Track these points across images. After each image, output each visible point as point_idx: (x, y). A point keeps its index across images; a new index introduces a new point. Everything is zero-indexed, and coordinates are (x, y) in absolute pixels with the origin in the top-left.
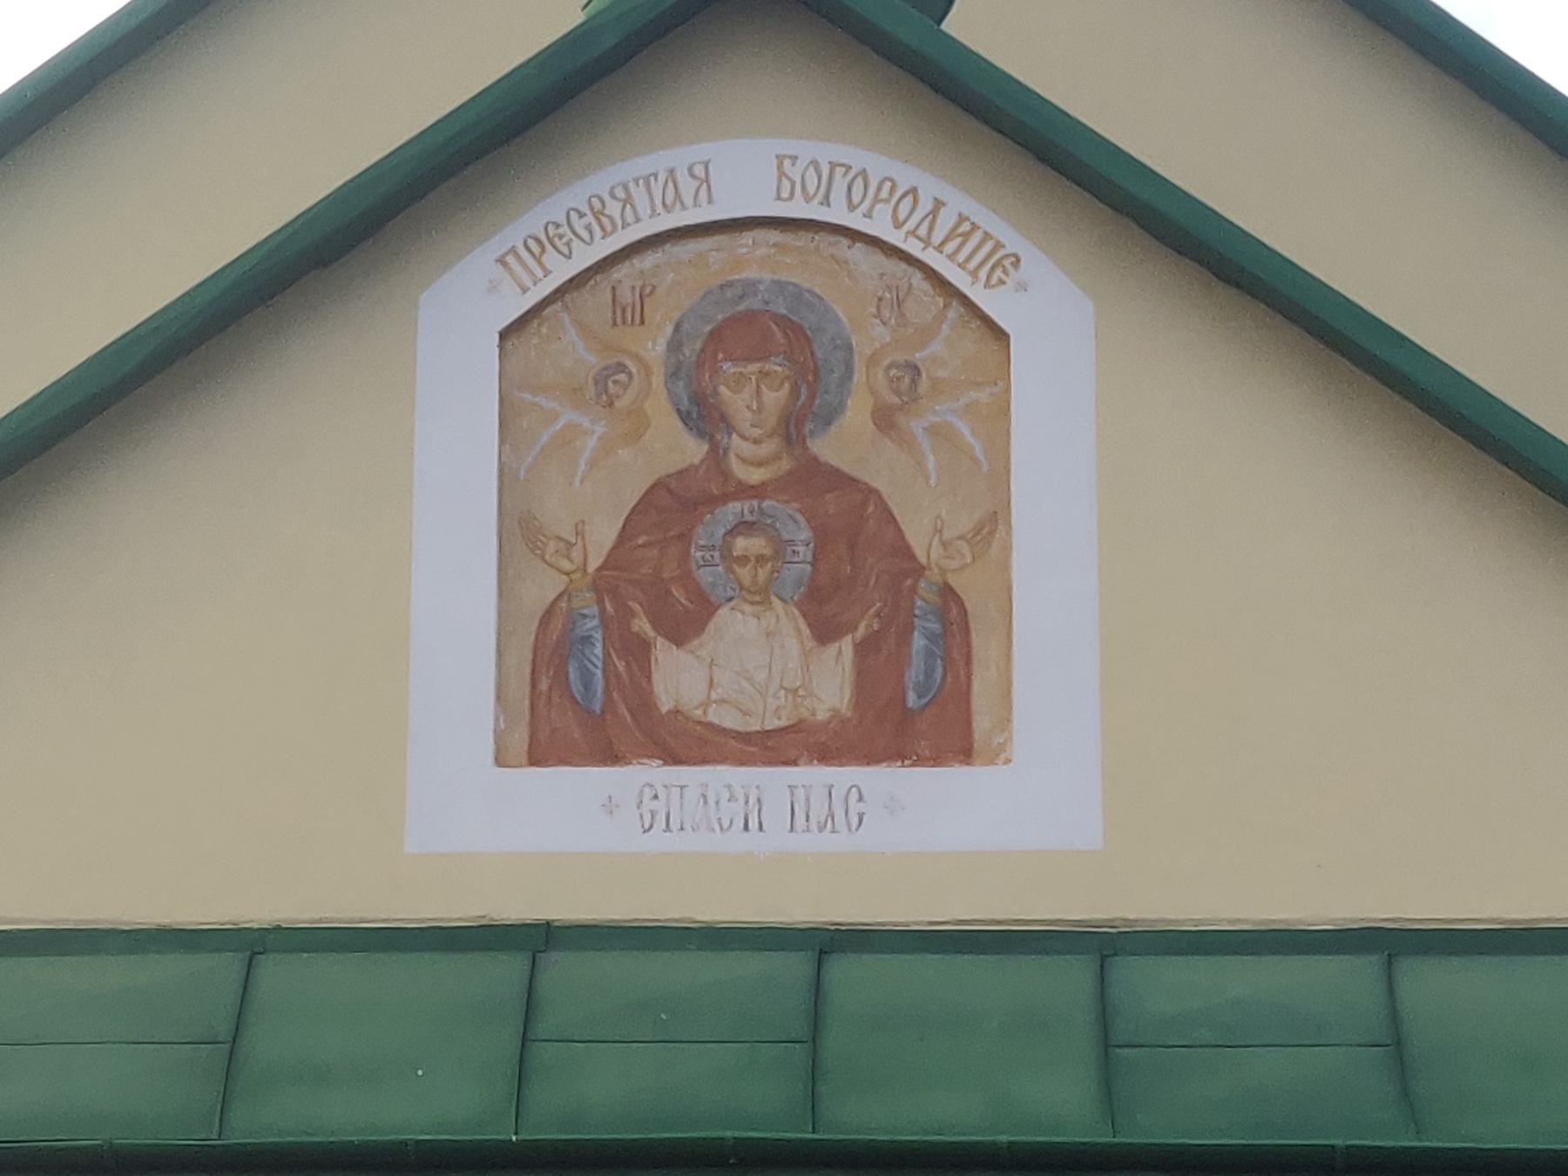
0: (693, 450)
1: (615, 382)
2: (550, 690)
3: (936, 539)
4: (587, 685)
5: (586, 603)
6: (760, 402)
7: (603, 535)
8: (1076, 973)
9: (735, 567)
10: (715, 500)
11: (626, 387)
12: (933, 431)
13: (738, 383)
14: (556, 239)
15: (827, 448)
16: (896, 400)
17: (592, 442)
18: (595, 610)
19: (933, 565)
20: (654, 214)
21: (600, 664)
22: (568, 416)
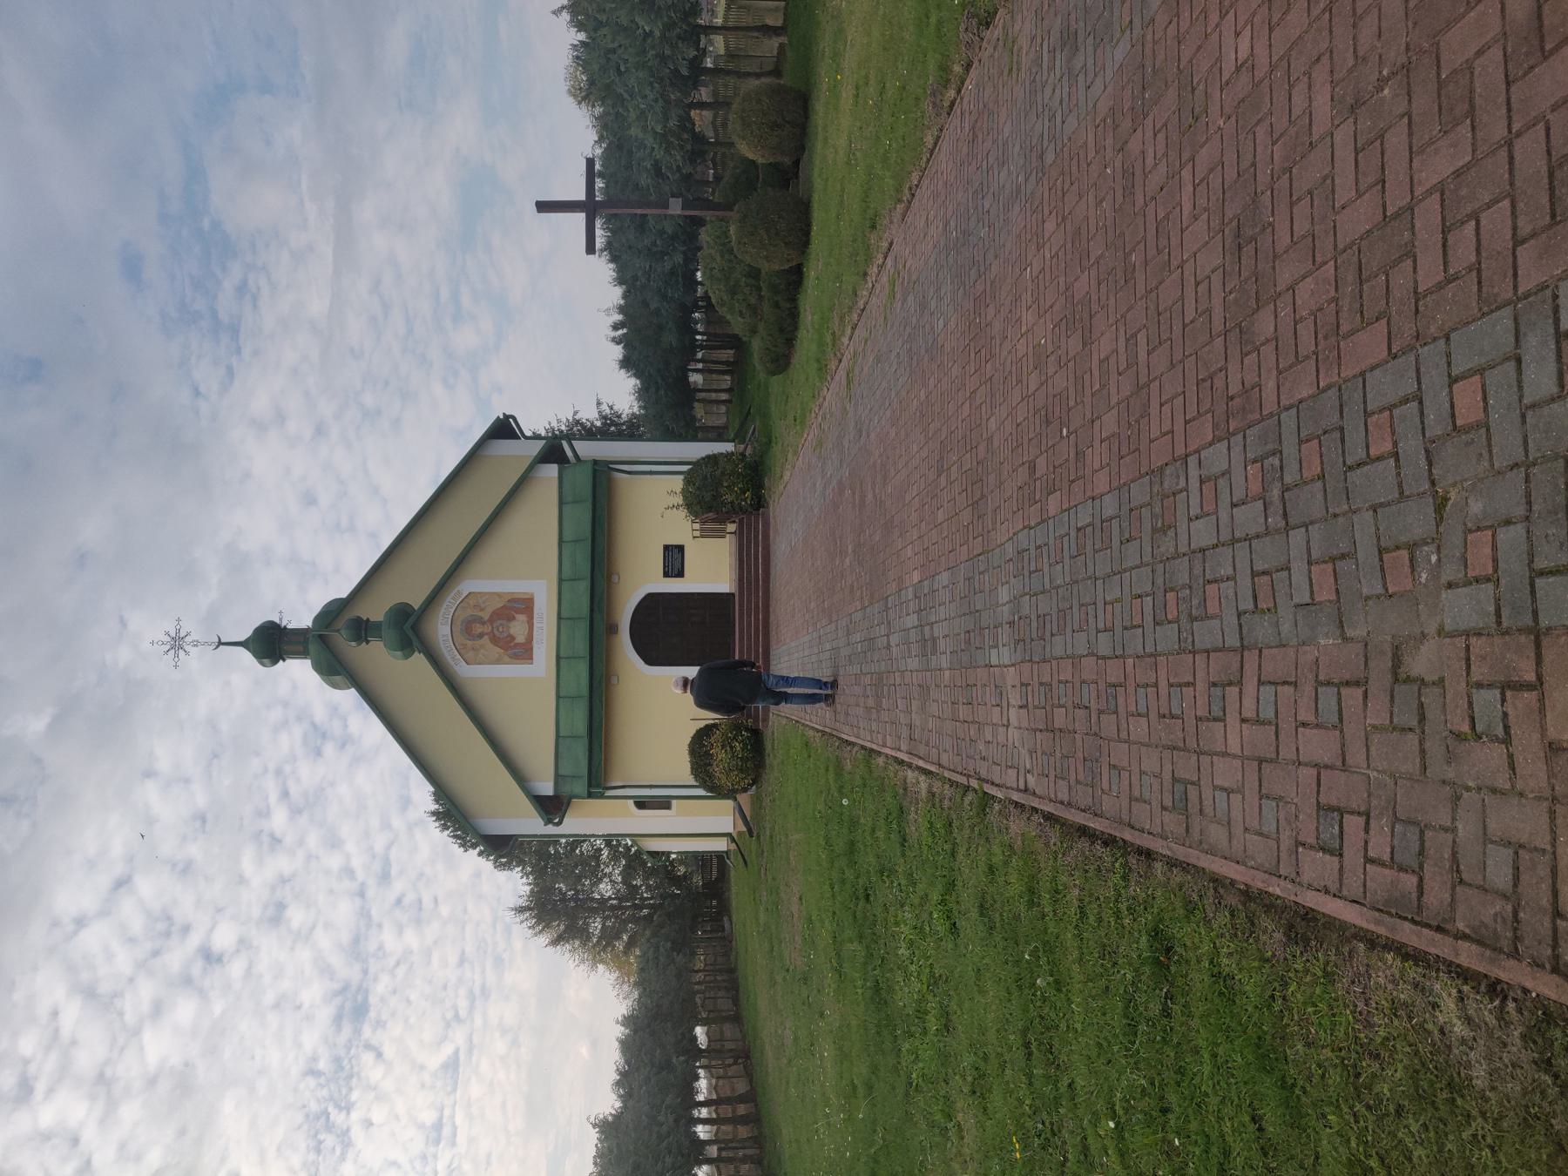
0: (486, 637)
10: (494, 636)
15: (486, 618)
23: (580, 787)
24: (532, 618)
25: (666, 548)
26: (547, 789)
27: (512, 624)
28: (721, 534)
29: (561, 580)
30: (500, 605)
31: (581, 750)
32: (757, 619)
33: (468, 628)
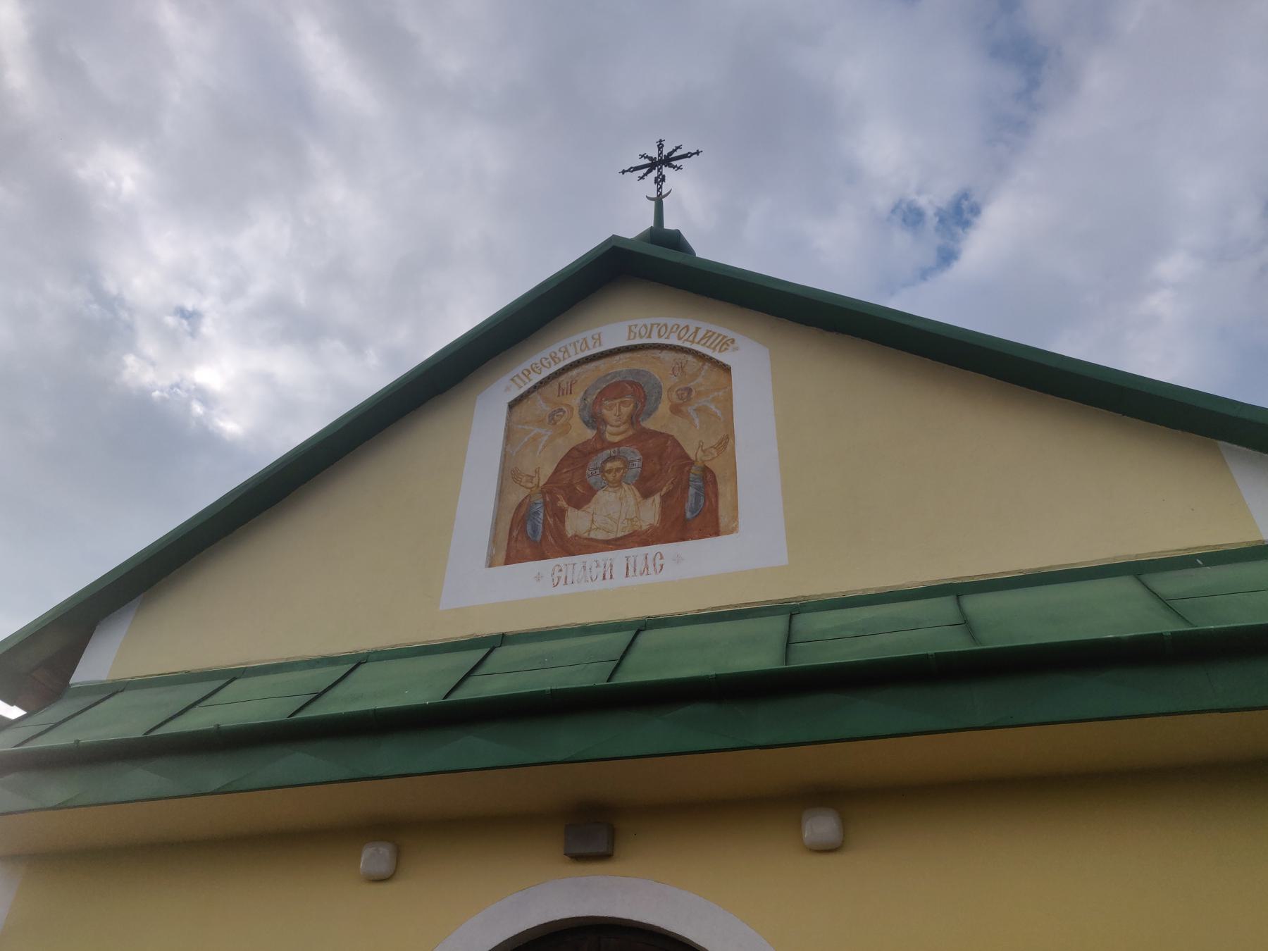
0: (590, 434)
1: (557, 416)
2: (517, 535)
3: (700, 451)
4: (535, 531)
5: (538, 499)
6: (620, 411)
7: (548, 470)
9: (606, 474)
10: (596, 451)
11: (562, 416)
12: (698, 410)
13: (610, 408)
14: (535, 369)
15: (649, 424)
16: (682, 402)
17: (545, 438)
18: (542, 500)
19: (698, 460)
20: (577, 353)
21: (541, 522)
22: (537, 430)
24: (645, 543)
27: (630, 494)
30: (691, 453)
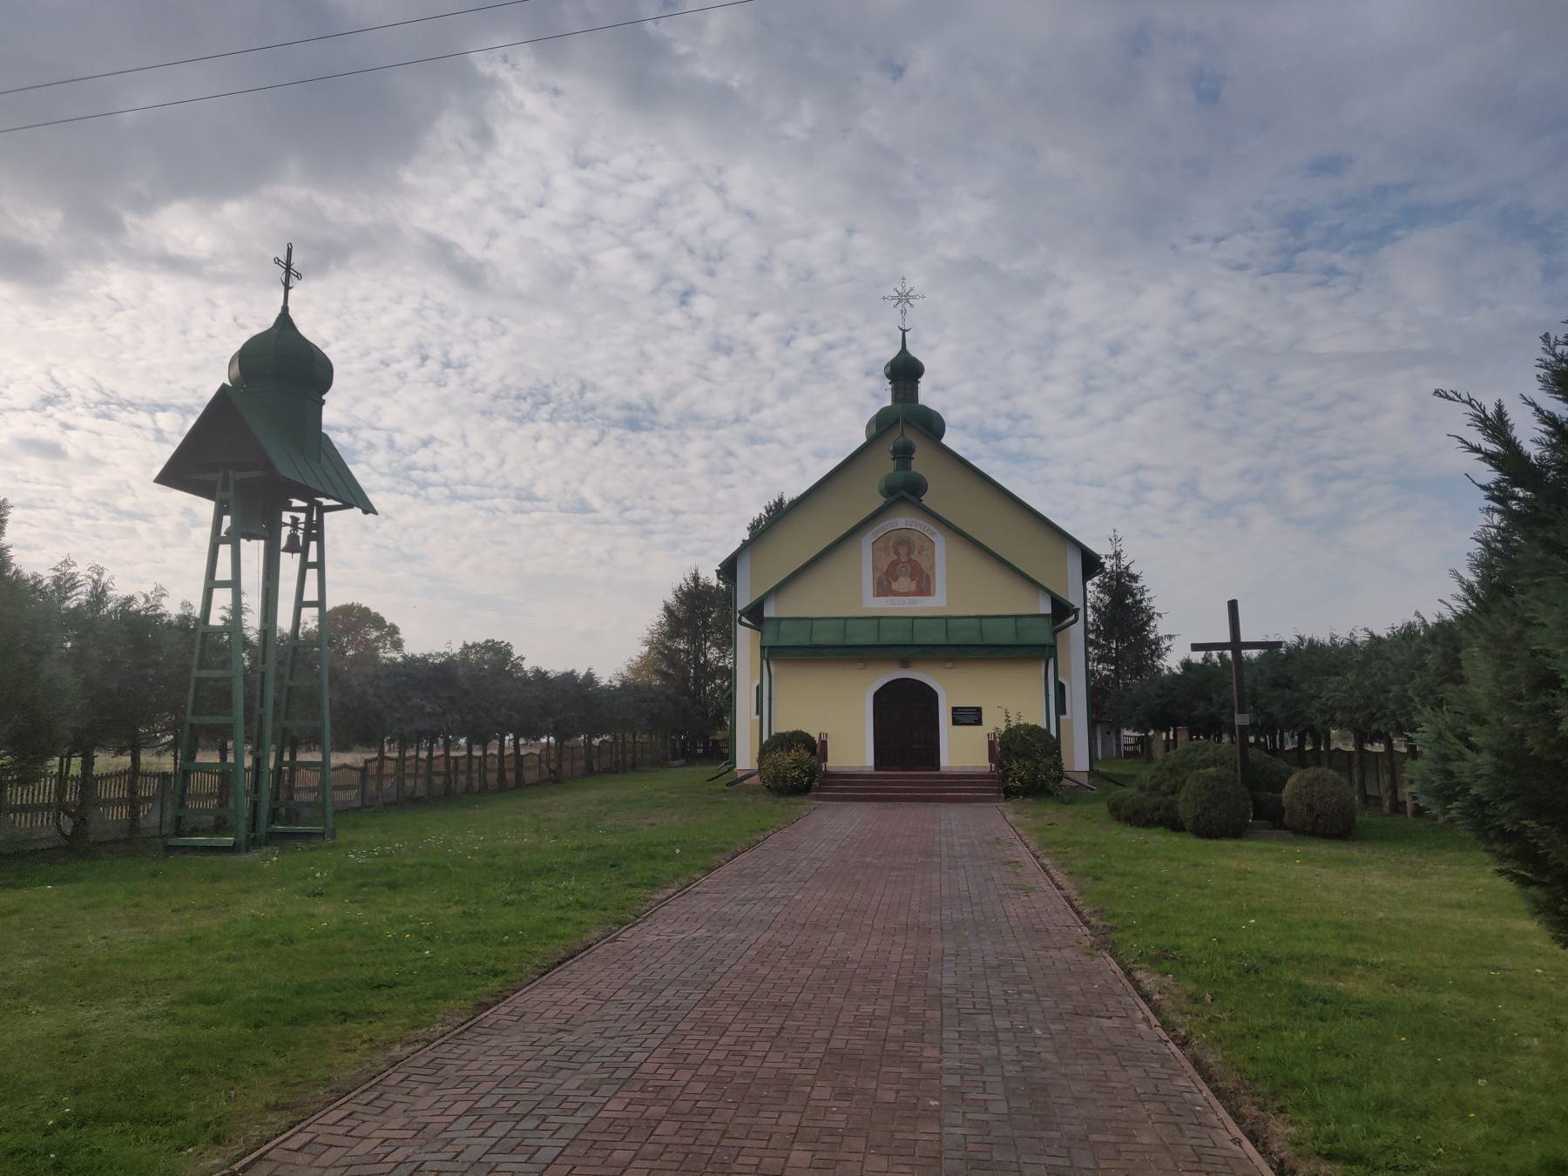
0: (896, 557)
7: (885, 568)
8: (942, 622)
15: (912, 557)
23: (770, 640)
24: (913, 595)
25: (979, 710)
26: (769, 611)
28: (991, 759)
29: (947, 618)
30: (924, 568)
31: (800, 638)
32: (907, 790)
33: (903, 541)
